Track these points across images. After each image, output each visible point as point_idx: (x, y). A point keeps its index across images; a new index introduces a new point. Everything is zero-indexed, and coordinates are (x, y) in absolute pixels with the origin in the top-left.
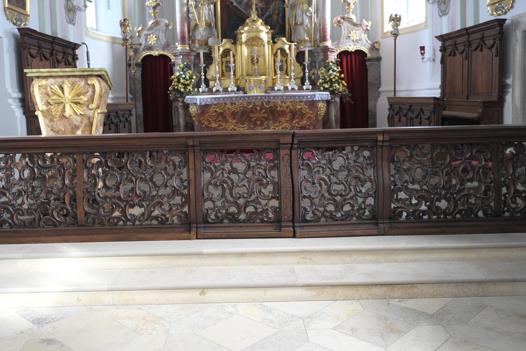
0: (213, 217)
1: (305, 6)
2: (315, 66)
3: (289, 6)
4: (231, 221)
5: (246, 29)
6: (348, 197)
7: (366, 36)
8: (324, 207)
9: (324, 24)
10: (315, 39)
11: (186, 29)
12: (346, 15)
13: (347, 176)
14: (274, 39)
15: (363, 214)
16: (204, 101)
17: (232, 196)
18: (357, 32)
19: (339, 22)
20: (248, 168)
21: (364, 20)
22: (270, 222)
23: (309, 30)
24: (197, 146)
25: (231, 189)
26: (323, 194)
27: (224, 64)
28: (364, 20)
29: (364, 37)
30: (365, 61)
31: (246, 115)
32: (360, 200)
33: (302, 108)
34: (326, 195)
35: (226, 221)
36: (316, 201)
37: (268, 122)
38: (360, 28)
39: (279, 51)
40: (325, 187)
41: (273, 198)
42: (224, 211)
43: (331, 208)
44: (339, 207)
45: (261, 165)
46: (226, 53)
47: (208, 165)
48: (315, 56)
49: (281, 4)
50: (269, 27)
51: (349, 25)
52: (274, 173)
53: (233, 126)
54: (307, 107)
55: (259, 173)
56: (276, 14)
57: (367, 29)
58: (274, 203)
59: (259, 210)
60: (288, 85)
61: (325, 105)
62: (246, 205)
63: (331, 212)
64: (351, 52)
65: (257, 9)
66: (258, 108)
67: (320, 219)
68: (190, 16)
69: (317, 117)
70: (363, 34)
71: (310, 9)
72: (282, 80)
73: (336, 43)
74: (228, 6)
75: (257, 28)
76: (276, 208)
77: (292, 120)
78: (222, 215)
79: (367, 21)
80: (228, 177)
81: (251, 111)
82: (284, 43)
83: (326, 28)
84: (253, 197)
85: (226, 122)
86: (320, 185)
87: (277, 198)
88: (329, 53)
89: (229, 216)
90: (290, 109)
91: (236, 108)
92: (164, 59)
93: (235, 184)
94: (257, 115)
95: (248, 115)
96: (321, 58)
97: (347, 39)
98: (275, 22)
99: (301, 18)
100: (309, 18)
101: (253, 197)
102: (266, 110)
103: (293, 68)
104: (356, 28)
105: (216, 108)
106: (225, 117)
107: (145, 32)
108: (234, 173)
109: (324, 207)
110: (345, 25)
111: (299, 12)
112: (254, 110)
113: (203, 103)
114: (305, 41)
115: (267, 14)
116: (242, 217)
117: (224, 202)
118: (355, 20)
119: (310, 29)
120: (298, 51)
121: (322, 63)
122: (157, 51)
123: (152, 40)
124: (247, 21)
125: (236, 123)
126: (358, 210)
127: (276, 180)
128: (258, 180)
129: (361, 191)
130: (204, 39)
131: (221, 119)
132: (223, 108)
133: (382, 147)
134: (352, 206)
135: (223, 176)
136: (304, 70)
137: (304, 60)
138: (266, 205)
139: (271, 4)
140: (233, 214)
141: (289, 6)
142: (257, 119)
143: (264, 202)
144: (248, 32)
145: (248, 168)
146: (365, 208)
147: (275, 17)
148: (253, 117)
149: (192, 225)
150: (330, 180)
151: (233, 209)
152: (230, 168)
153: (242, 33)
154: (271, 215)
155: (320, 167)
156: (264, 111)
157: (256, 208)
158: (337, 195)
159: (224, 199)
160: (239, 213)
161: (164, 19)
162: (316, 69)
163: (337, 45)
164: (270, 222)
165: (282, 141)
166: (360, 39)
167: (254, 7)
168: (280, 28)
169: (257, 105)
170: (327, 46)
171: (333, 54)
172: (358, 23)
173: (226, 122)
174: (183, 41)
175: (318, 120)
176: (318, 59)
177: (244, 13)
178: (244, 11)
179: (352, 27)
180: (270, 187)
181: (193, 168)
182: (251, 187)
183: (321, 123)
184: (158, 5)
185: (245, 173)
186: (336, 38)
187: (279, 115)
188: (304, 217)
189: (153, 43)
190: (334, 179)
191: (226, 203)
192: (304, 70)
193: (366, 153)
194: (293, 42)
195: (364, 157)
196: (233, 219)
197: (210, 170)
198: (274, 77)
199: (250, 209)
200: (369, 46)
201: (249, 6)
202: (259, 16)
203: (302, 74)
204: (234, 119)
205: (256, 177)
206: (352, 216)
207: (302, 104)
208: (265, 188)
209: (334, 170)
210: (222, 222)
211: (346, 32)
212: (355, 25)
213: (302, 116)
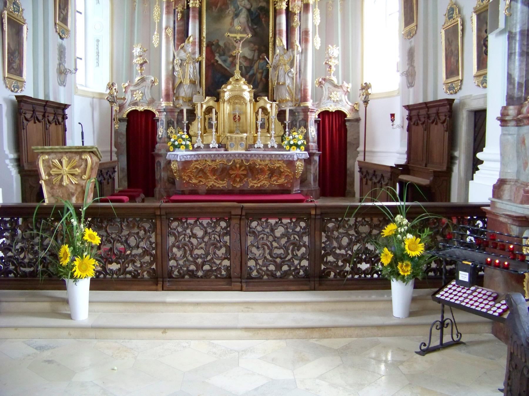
0: (176, 273)
1: (288, 67)
2: (296, 125)
3: (272, 66)
4: (191, 276)
5: (229, 87)
6: (287, 259)
7: (346, 97)
8: (267, 267)
9: (306, 86)
10: (297, 99)
11: (171, 86)
12: (327, 77)
13: (286, 242)
14: (256, 97)
15: (299, 273)
16: (183, 157)
17: (192, 256)
18: (338, 93)
19: (320, 83)
20: (206, 234)
21: (344, 82)
22: (223, 278)
23: (290, 90)
24: (164, 215)
25: (191, 251)
26: (265, 257)
27: (207, 121)
28: (344, 82)
29: (345, 98)
30: (345, 121)
31: (226, 172)
32: (296, 262)
33: (280, 166)
34: (268, 257)
35: (187, 277)
36: (260, 262)
37: (247, 180)
38: (340, 90)
39: (260, 110)
40: (267, 251)
41: (225, 258)
42: (185, 269)
43: (272, 267)
44: (279, 267)
45: (216, 232)
46: (209, 110)
47: (173, 231)
48: (295, 116)
49: (265, 64)
50: (252, 86)
51: (330, 86)
52: (227, 238)
53: (213, 182)
54: (285, 165)
55: (215, 238)
56: (260, 73)
57: (347, 91)
58: (226, 263)
59: (214, 268)
60: (269, 143)
61: (303, 164)
62: (203, 264)
63: (271, 271)
64: (332, 112)
65: (241, 68)
66: (238, 166)
67: (263, 276)
68: (175, 74)
69: (294, 175)
70: (343, 96)
71: (292, 70)
72: (263, 137)
73: (317, 103)
74: (213, 64)
75: (240, 87)
76: (228, 267)
77: (270, 178)
78: (183, 272)
79: (348, 83)
80: (189, 241)
81: (231, 168)
82: (266, 102)
83: (307, 89)
84: (209, 258)
85: (207, 178)
86: (264, 249)
87: (229, 259)
88: (309, 113)
89: (189, 273)
90: (269, 167)
91: (216, 165)
92: (148, 114)
93: (194, 247)
94: (235, 172)
95: (228, 172)
96: (301, 117)
97: (328, 99)
98: (259, 80)
99: (283, 78)
100: (291, 79)
101: (209, 258)
102: (246, 167)
103: (273, 126)
104: (337, 89)
105: (197, 165)
106: (205, 174)
107: (132, 88)
108: (193, 238)
109: (267, 267)
110: (327, 85)
111: (281, 73)
112: (233, 167)
113: (183, 160)
114: (287, 101)
115: (251, 72)
116: (200, 274)
117: (185, 261)
118: (336, 82)
119: (292, 89)
120: (280, 110)
121: (303, 122)
122: (142, 106)
123: (138, 97)
124: (231, 80)
125: (216, 179)
126: (294, 270)
127: (228, 244)
128: (213, 244)
129: (297, 255)
130: (188, 96)
131: (201, 175)
132: (204, 165)
133: (315, 219)
134: (289, 266)
135: (185, 240)
136: (285, 128)
137: (285, 120)
138: (220, 264)
139: (255, 63)
140: (192, 271)
141: (272, 66)
142: (236, 176)
143: (218, 262)
144: (231, 90)
145: (206, 234)
146: (300, 269)
147: (259, 76)
148: (232, 174)
149: (159, 279)
150: (272, 245)
151: (192, 267)
152: (191, 234)
153: (225, 92)
154: (224, 273)
155: (264, 234)
156: (243, 168)
157: (211, 267)
158: (277, 258)
159: (185, 259)
160: (197, 270)
161: (151, 76)
162: (296, 127)
163: (318, 106)
164: (223, 278)
165: (233, 213)
166: (341, 101)
167: (238, 67)
168: (262, 87)
169: (237, 163)
170: (308, 107)
171: (313, 114)
173: (207, 178)
174: (168, 97)
175: (296, 178)
176: (299, 118)
177: (228, 71)
178: (228, 69)
179: (333, 88)
180: (223, 250)
181: (160, 233)
182: (207, 249)
183: (299, 181)
184: (145, 62)
185: (203, 238)
186: (318, 99)
187: (258, 173)
188: (250, 275)
189: (138, 100)
190: (275, 244)
191: (187, 263)
192: (285, 128)
193: (303, 224)
194: (275, 101)
195: (301, 227)
196: (192, 274)
197: (174, 235)
198: (255, 135)
199: (207, 267)
201: (233, 64)
202: (242, 75)
203: (283, 133)
204: (214, 175)
205: (212, 242)
206: (290, 275)
207: (280, 162)
208: (219, 250)
209: (276, 237)
210: (183, 277)
211: (327, 93)
212: (336, 86)
213: (281, 173)
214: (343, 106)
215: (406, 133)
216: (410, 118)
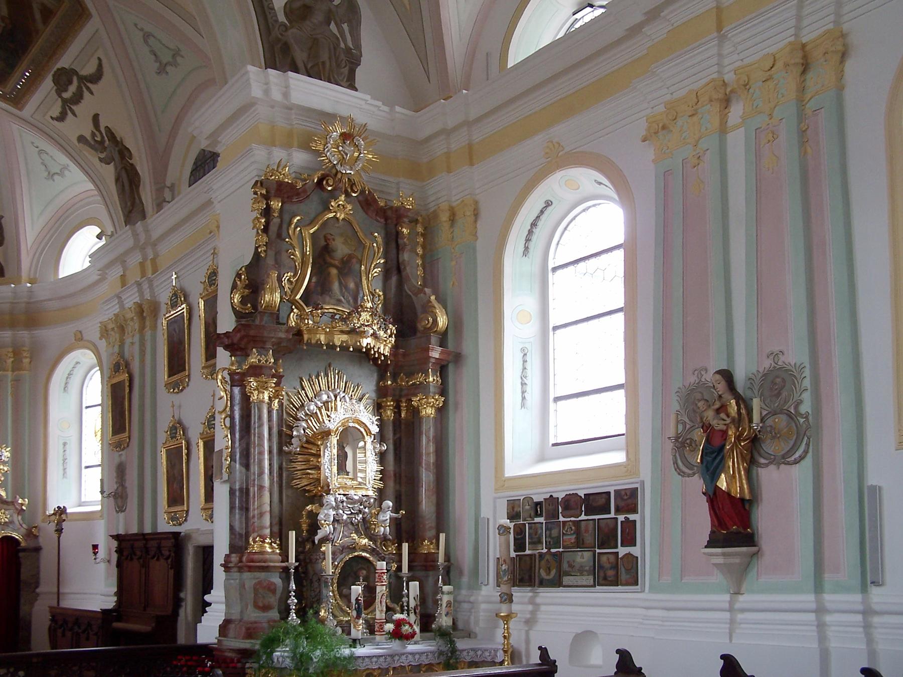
7: (20, 518)
29: (18, 519)
70: (15, 516)
104: (5, 506)
172: (10, 500)
200: (23, 531)
214: (14, 530)
215: (115, 570)
216: (119, 551)
